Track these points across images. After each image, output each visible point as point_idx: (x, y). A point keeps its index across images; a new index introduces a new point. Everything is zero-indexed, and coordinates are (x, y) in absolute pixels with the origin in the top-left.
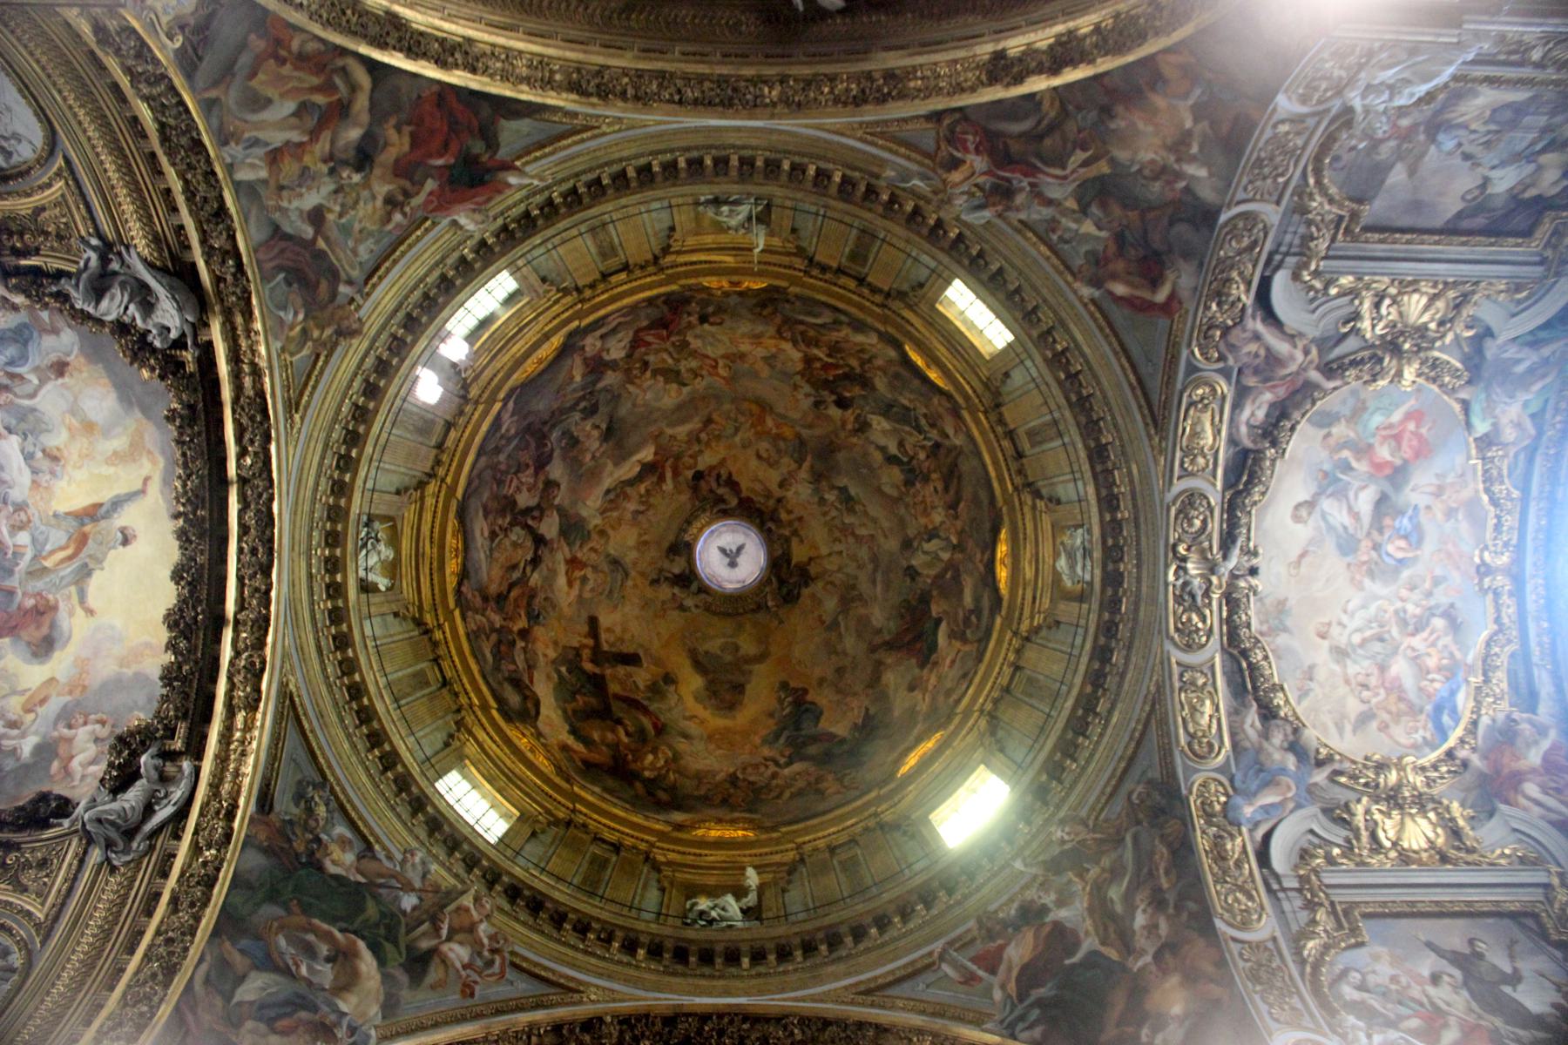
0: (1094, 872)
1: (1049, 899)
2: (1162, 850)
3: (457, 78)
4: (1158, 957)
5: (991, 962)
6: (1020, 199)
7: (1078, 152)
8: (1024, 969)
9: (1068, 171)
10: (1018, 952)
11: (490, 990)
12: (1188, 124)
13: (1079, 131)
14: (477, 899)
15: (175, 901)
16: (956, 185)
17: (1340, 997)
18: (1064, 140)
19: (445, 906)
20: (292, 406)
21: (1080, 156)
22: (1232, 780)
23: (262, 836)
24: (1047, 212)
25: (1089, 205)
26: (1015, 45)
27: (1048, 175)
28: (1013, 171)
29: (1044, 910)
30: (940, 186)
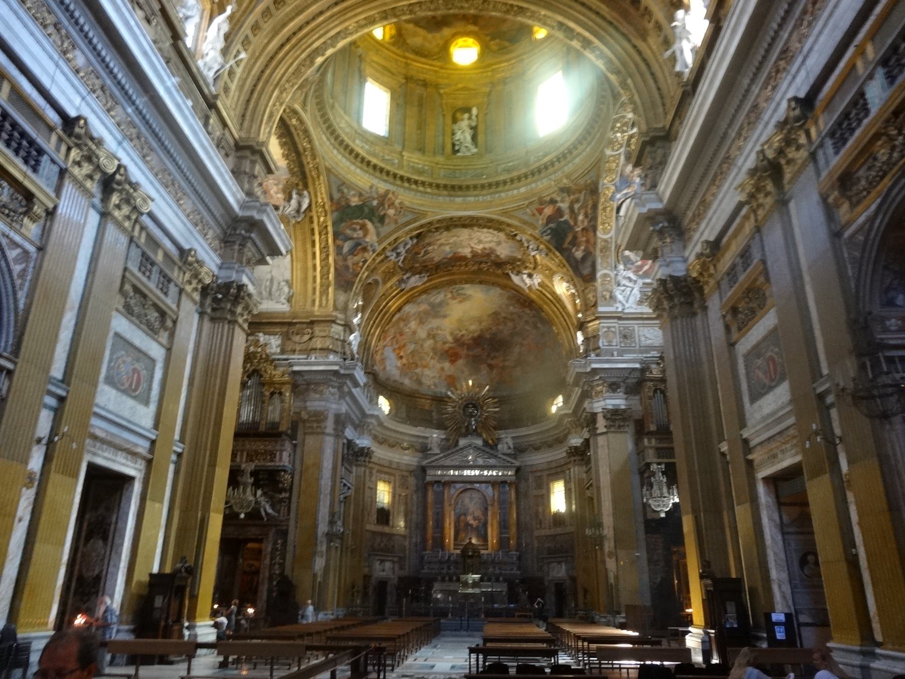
0: (572, 197)
1: (559, 199)
2: (590, 203)
3: (341, 44)
4: (583, 229)
5: (540, 211)
8: (549, 217)
10: (548, 211)
11: (402, 220)
14: (393, 193)
15: (320, 234)
17: (622, 254)
19: (384, 200)
20: (304, 104)
22: (616, 187)
23: (334, 208)
26: (572, 25)
29: (556, 202)
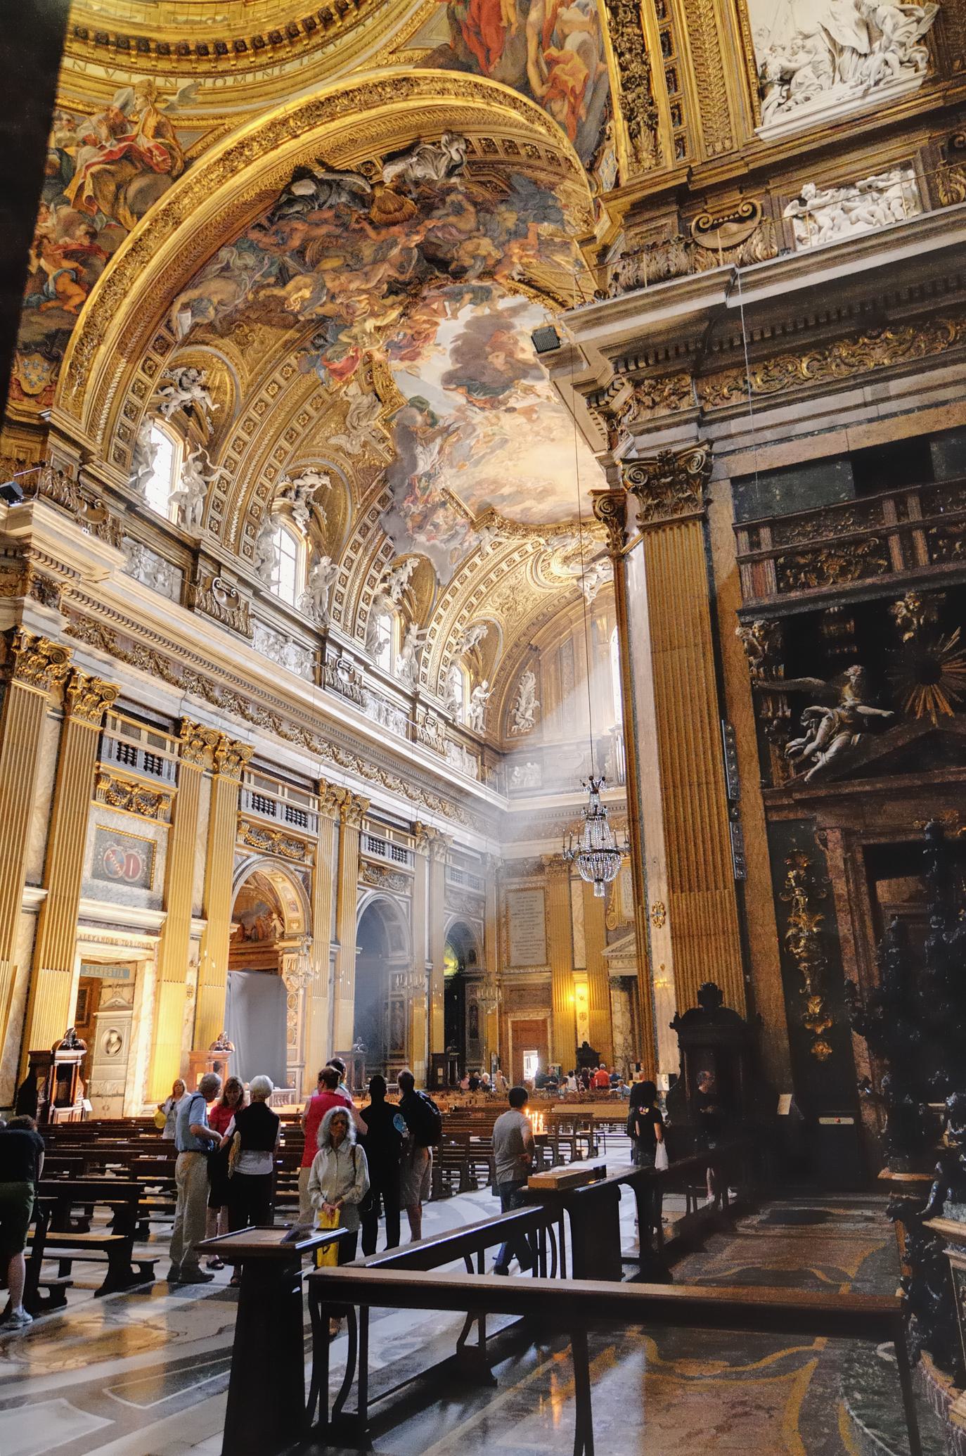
6: (104, 131)
7: (91, 194)
9: (88, 175)
12: (43, 262)
13: (99, 210)
16: (149, 114)
18: (105, 198)
21: (88, 191)
24: (82, 133)
25: (61, 159)
27: (99, 163)
28: (121, 150)
30: (158, 105)
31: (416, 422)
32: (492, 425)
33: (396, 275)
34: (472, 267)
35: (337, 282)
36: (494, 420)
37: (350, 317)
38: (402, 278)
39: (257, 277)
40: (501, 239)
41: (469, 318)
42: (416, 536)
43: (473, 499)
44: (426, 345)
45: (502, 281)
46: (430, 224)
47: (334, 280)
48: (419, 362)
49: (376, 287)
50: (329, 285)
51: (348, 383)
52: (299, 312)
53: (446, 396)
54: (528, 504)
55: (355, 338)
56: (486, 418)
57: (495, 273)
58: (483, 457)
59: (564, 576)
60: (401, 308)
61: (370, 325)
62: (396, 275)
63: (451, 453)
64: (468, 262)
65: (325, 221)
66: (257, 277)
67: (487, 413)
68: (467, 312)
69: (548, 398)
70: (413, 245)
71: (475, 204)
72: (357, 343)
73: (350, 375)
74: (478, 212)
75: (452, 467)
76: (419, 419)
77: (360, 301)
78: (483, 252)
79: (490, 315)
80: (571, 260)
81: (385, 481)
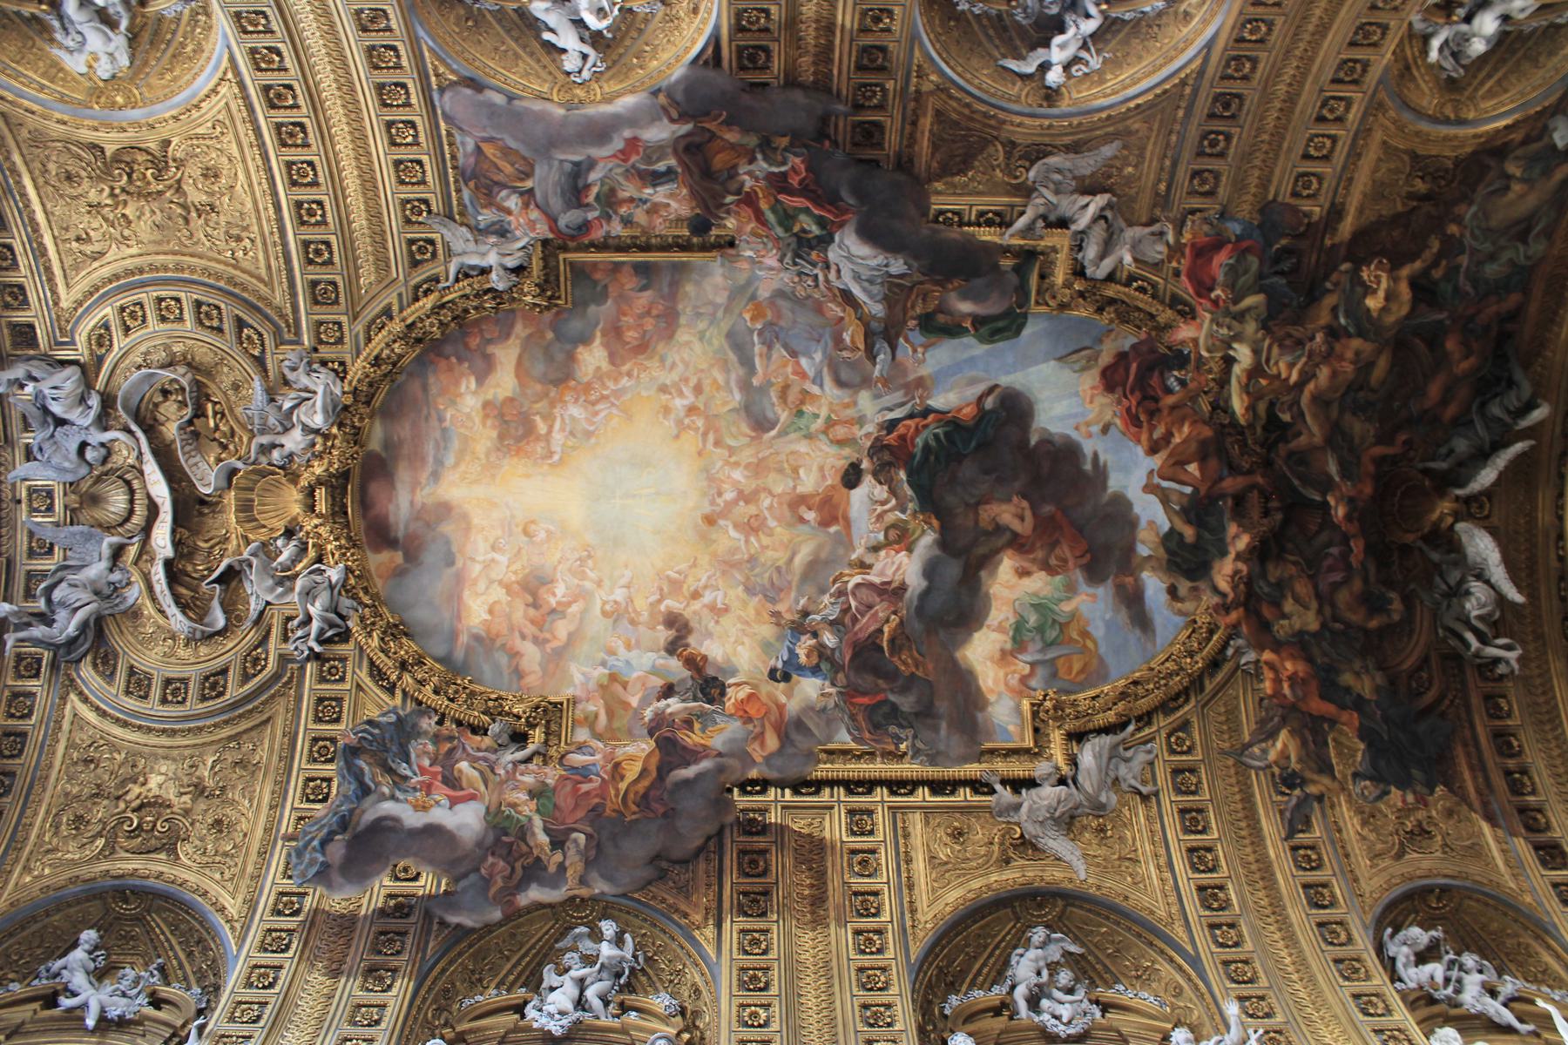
31: (965, 297)
32: (830, 424)
33: (1293, 445)
34: (1264, 575)
35: (1349, 355)
36: (840, 432)
37: (1281, 333)
38: (1283, 449)
39: (1464, 260)
40: (1316, 651)
41: (1137, 509)
42: (686, 128)
43: (629, 282)
44: (1118, 409)
45: (1234, 616)
46: (1357, 546)
47: (1357, 353)
48: (1091, 379)
49: (1297, 402)
50: (1356, 343)
51: (1176, 250)
52: (1356, 271)
53: (973, 382)
54: (504, 382)
55: (1240, 317)
56: (861, 421)
57: (1247, 610)
58: (747, 362)
59: (119, 342)
60: (1242, 422)
61: (1243, 355)
62: (1293, 445)
63: (819, 309)
64: (1274, 572)
65: (1444, 402)
66: (1464, 260)
67: (870, 428)
68: (1152, 515)
69: (863, 566)
70: (1331, 501)
71: (1381, 631)
72: (1227, 313)
73: (1185, 264)
74: (1366, 632)
75: (780, 294)
76: (966, 307)
77: (1291, 366)
78: (1289, 605)
79: (1131, 549)
80: (1294, 764)
81: (904, 163)
